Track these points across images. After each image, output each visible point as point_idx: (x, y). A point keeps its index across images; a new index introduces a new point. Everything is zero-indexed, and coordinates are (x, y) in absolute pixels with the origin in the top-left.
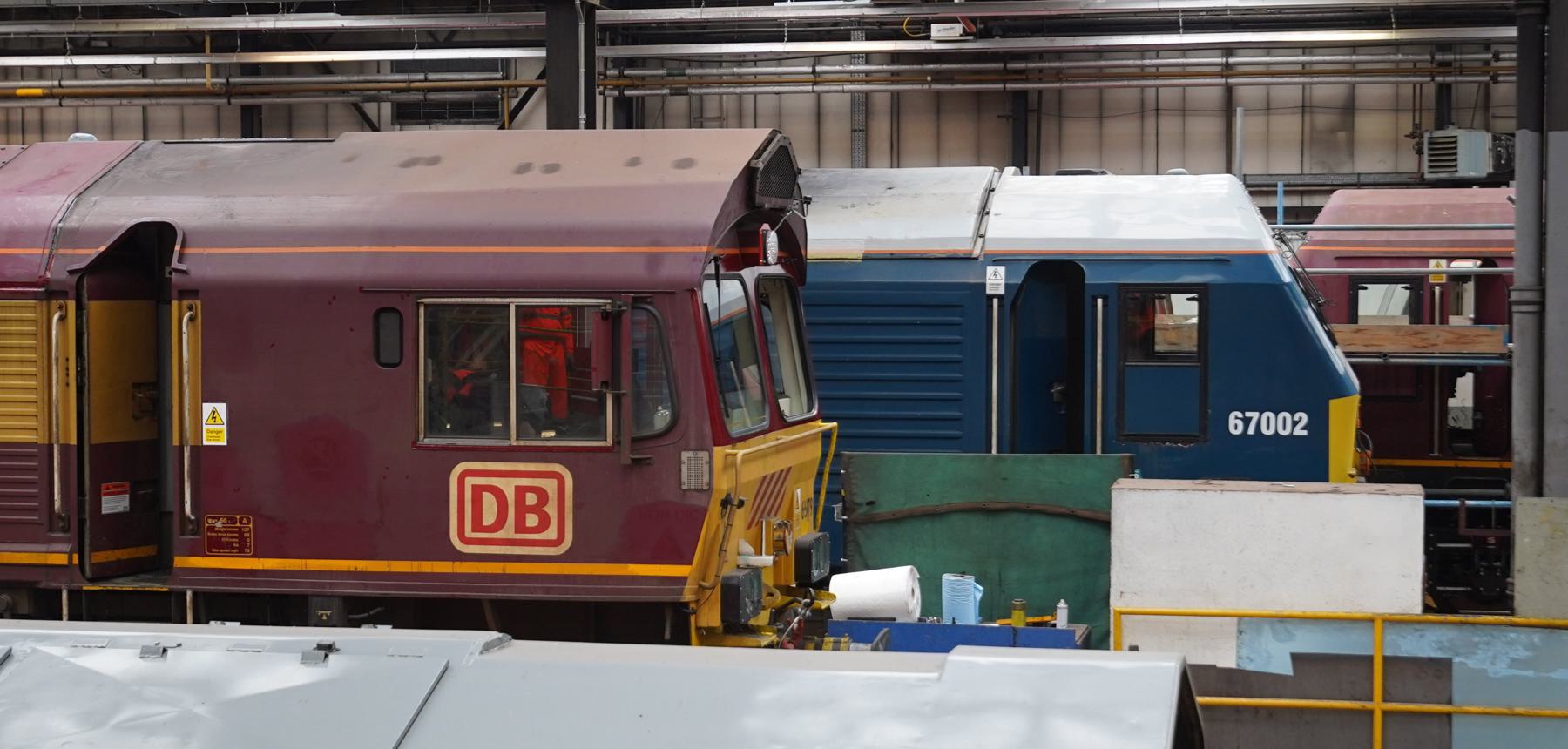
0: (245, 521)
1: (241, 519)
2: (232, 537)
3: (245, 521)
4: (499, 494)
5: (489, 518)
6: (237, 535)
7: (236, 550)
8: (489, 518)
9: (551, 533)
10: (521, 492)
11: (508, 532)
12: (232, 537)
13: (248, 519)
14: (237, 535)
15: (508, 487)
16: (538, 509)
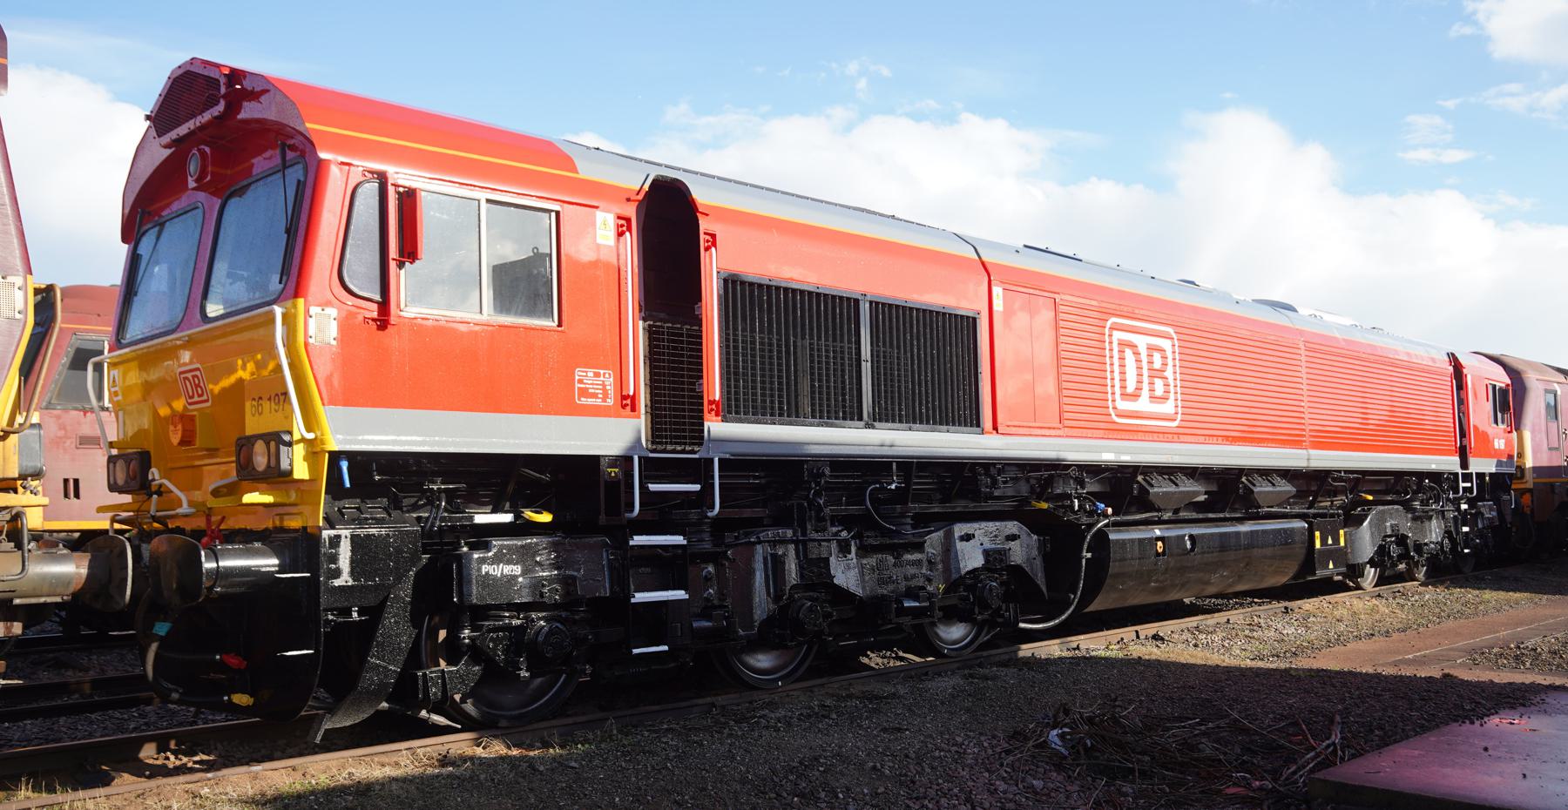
0: (607, 376)
1: (604, 374)
2: (597, 389)
3: (607, 376)
4: (187, 378)
5: (191, 394)
6: (601, 387)
7: (600, 400)
8: (191, 394)
10: (193, 377)
11: (196, 399)
12: (597, 389)
13: (610, 374)
14: (601, 387)
15: (189, 375)
16: (198, 386)
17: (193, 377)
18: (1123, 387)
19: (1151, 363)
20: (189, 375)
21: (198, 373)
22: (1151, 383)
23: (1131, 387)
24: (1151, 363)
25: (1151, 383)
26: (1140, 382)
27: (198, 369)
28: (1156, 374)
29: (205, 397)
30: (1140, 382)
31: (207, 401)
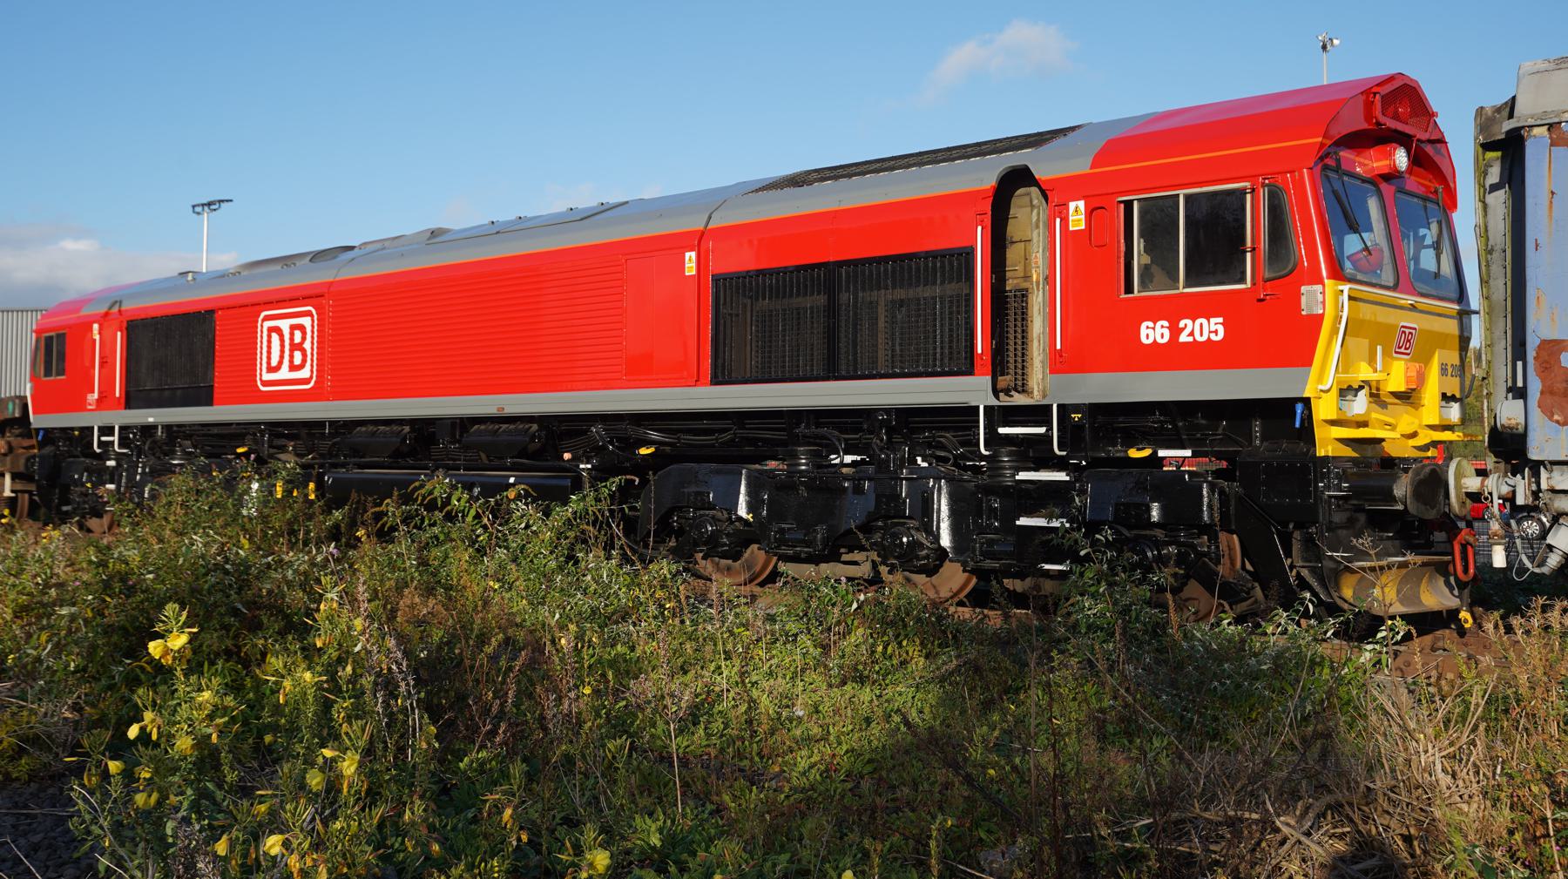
9: (1408, 351)
11: (1402, 350)
16: (1409, 341)
17: (1410, 333)
18: (269, 363)
19: (292, 339)
20: (1407, 331)
21: (1413, 331)
22: (292, 357)
23: (274, 363)
24: (292, 339)
25: (292, 357)
26: (282, 357)
27: (1415, 329)
28: (295, 347)
29: (1408, 351)
30: (282, 357)
31: (1408, 354)
